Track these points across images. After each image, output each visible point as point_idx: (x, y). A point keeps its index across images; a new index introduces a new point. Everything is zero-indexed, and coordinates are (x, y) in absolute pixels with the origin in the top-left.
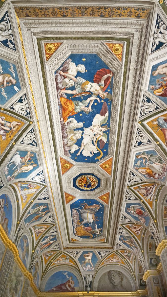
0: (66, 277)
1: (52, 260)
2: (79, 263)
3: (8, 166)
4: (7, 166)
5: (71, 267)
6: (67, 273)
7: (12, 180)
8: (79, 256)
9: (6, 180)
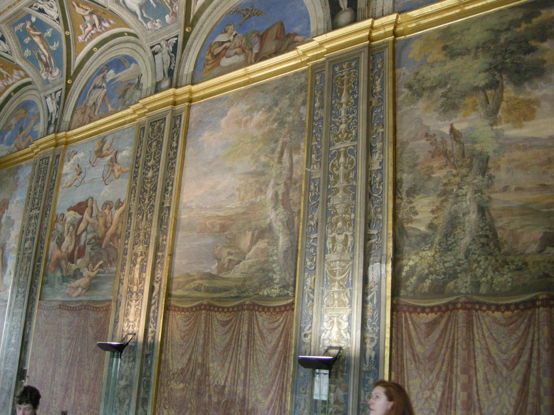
3: (146, 20)
4: (145, 25)
7: (177, 8)
9: (172, 26)
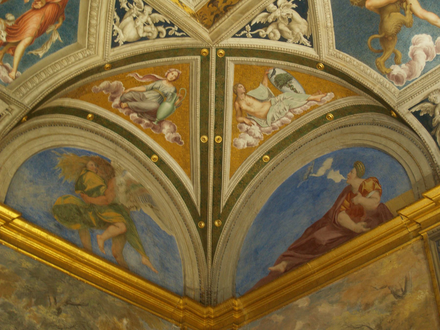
0: (331, 181)
1: (204, 131)
2: (356, 61)
5: (343, 120)
6: (329, 162)
8: (330, 23)
